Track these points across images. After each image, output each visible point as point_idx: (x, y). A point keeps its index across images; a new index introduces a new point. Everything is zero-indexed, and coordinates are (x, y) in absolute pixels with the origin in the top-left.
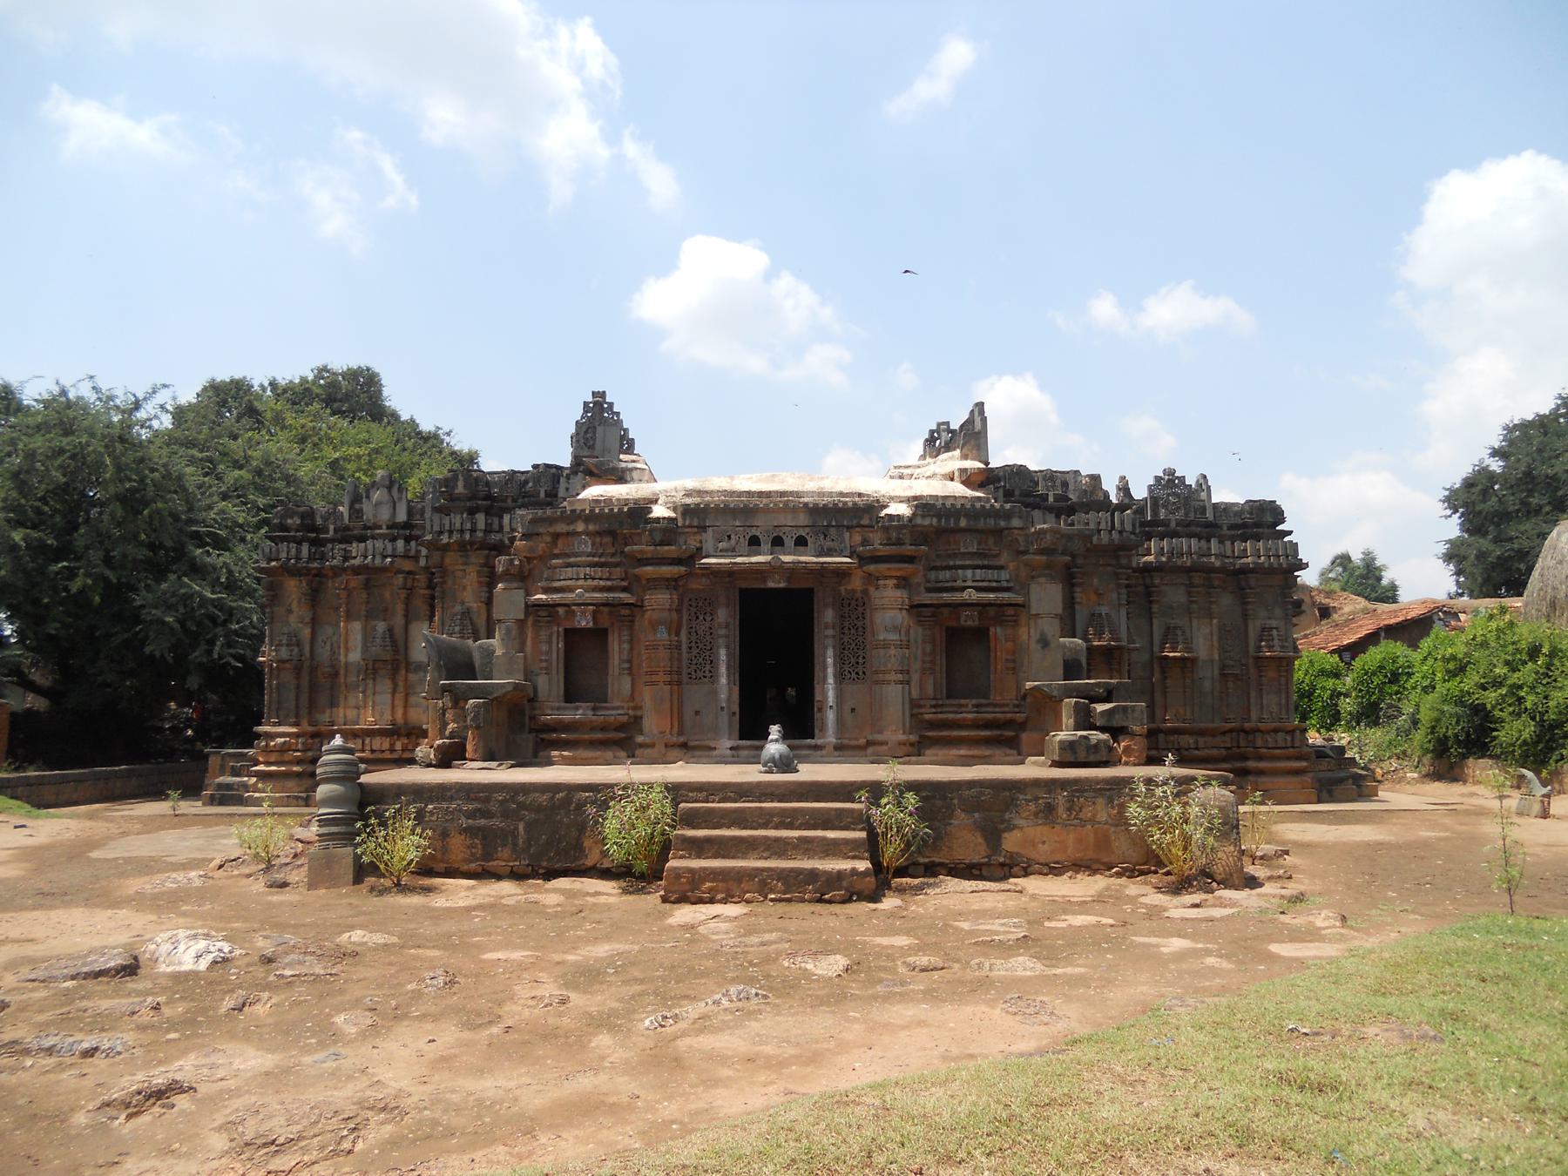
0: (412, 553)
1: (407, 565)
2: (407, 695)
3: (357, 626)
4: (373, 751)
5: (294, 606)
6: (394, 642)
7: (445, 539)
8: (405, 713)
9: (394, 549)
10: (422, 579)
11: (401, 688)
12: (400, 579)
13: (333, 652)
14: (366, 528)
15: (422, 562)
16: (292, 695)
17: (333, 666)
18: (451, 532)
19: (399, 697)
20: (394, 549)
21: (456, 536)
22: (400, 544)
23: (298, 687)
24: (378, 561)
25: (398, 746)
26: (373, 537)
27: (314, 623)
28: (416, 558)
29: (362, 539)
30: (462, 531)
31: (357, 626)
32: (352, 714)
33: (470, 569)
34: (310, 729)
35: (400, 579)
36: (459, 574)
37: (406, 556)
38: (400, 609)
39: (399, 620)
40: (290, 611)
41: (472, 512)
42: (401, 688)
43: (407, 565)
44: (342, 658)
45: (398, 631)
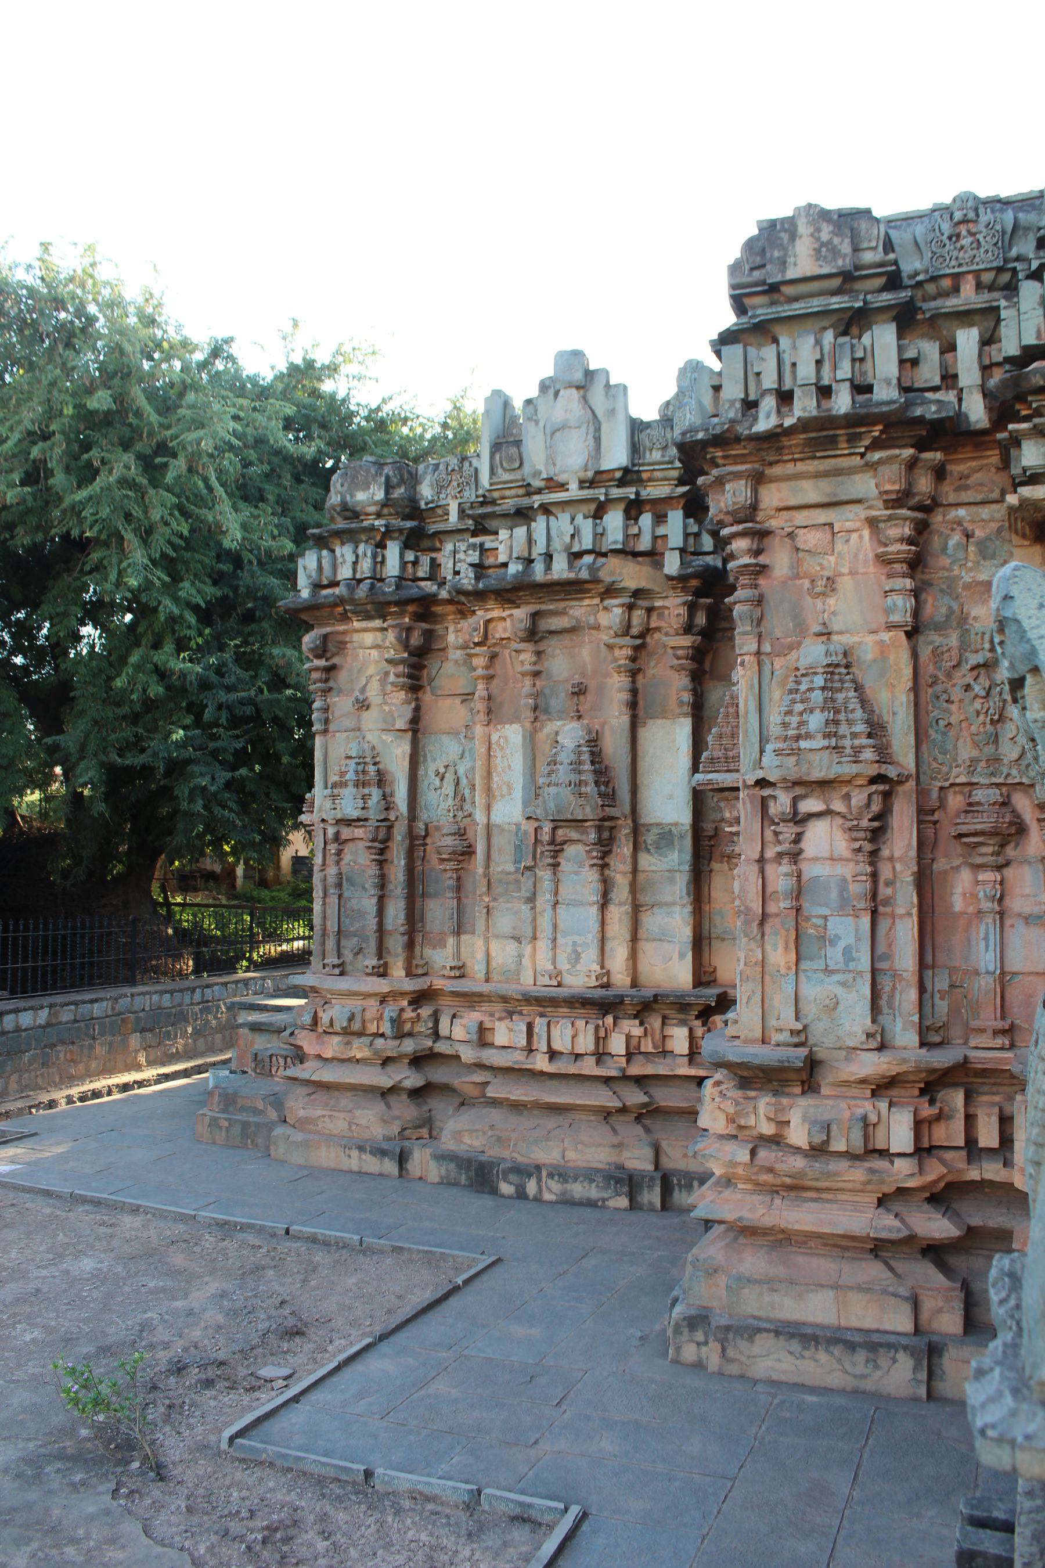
0: (645, 544)
1: (631, 575)
2: (636, 909)
3: (512, 736)
4: (553, 1055)
5: (373, 692)
6: (602, 774)
7: (765, 421)
8: (633, 955)
9: (599, 536)
10: (673, 606)
11: (621, 892)
12: (612, 615)
13: (460, 798)
14: (529, 491)
15: (672, 564)
16: (370, 904)
17: (461, 833)
18: (785, 398)
19: (618, 914)
20: (599, 536)
21: (805, 406)
22: (614, 520)
23: (382, 883)
24: (560, 569)
25: (617, 1045)
26: (546, 509)
27: (416, 727)
28: (654, 556)
29: (523, 515)
30: (825, 392)
31: (512, 736)
32: (503, 953)
33: (849, 518)
34: (410, 985)
35: (612, 615)
36: (809, 539)
37: (628, 553)
38: (617, 686)
39: (614, 718)
40: (363, 705)
41: (853, 323)
42: (621, 892)
43: (631, 575)
44: (480, 817)
45: (615, 746)
